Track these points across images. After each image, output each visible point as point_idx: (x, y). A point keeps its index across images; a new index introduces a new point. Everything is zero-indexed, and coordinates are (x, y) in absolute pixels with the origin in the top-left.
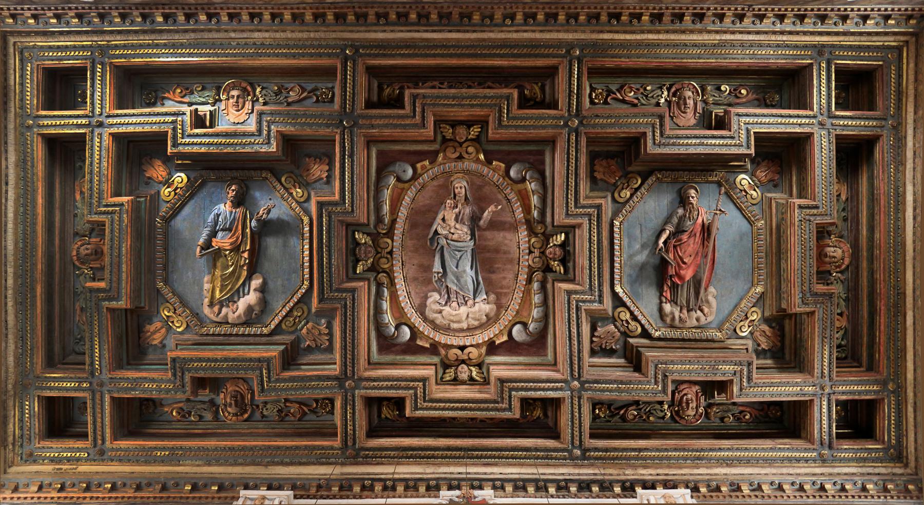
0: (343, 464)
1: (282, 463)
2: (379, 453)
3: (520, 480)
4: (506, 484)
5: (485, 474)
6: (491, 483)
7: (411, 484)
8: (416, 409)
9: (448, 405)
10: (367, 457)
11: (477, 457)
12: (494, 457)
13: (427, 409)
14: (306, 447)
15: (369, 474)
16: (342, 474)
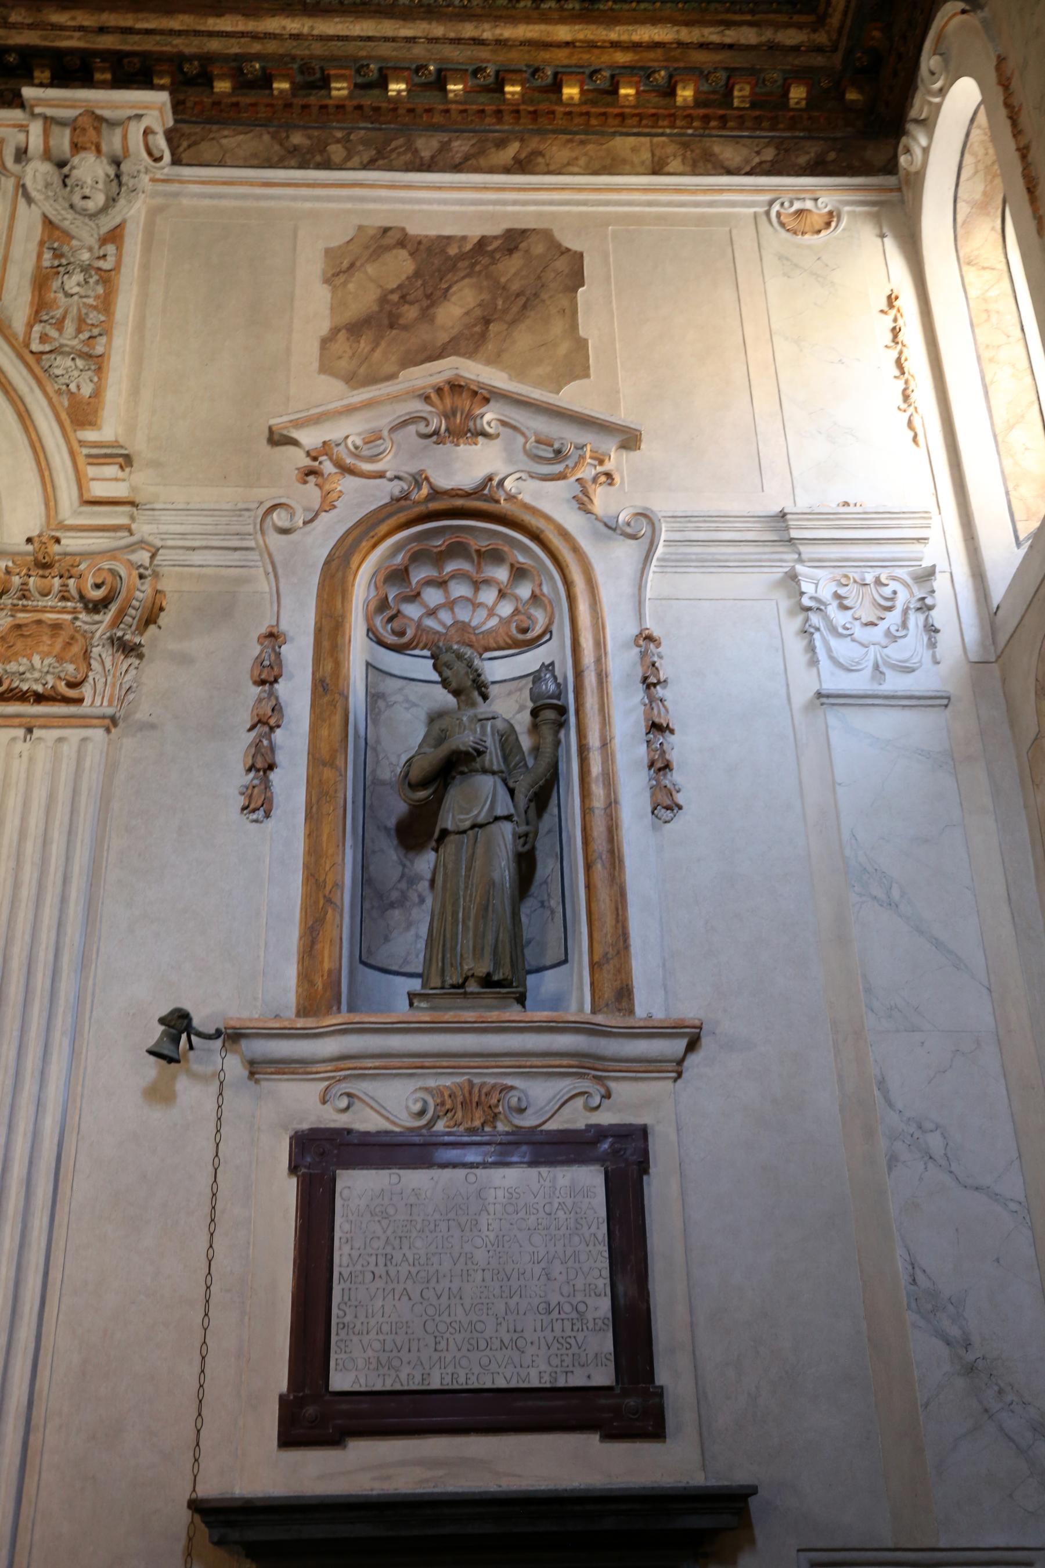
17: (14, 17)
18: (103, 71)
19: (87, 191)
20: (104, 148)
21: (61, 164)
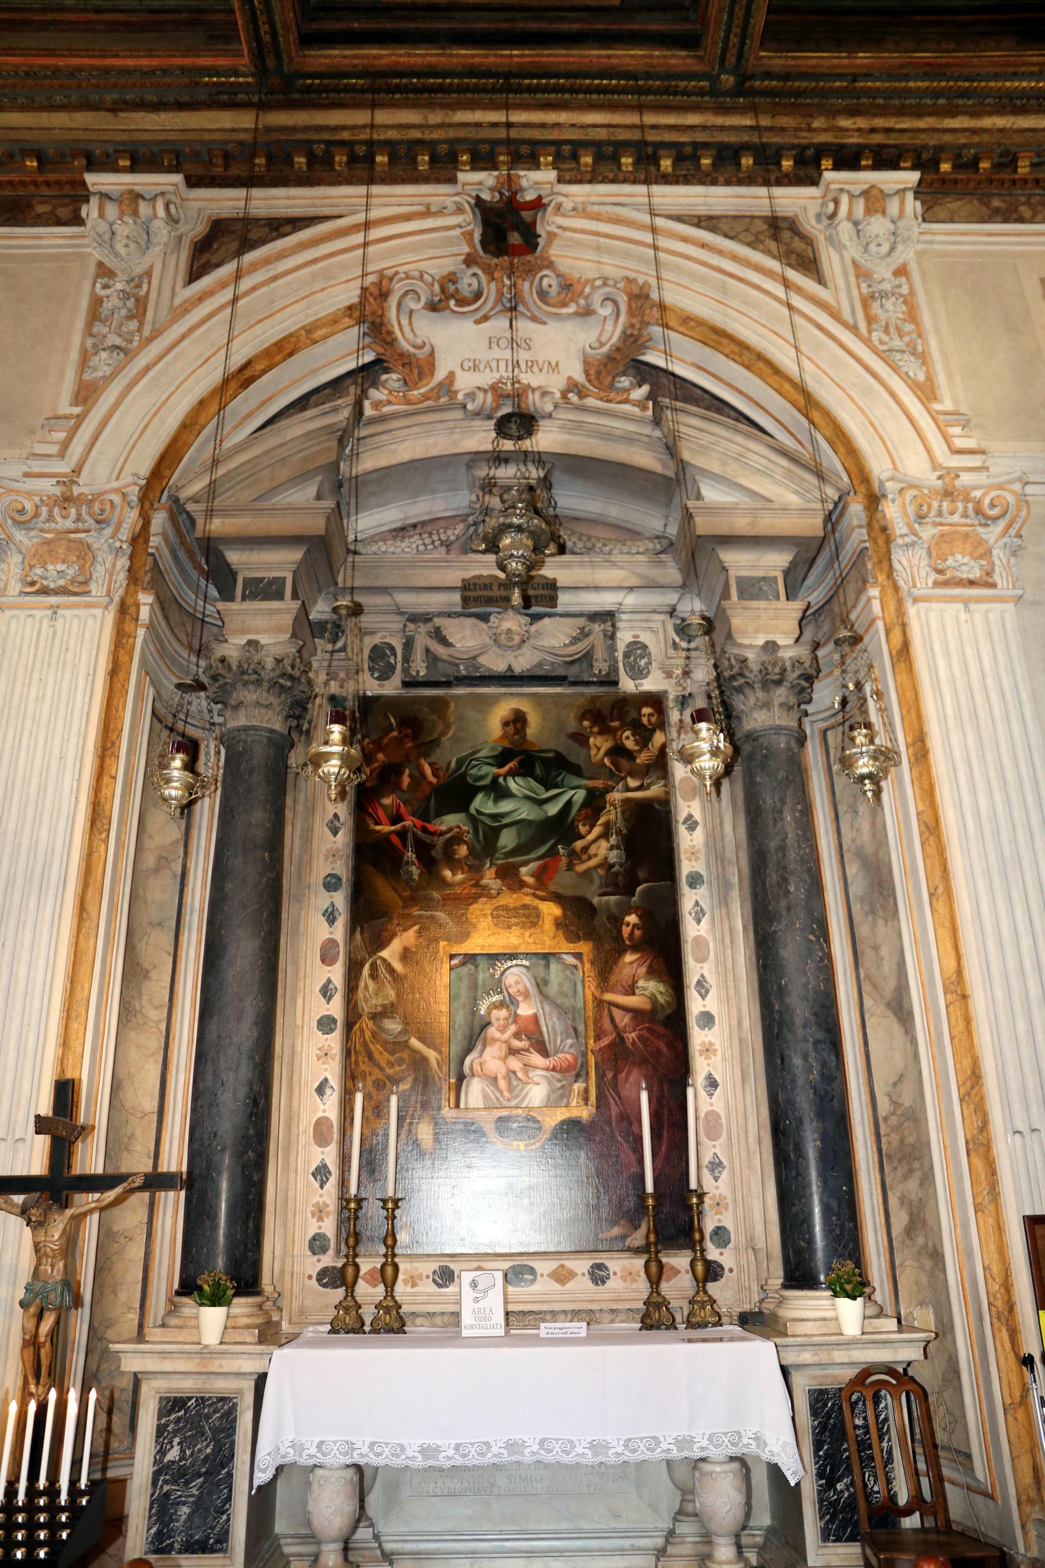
0: (262, 107)
1: (142, 106)
3: (609, 143)
5: (543, 126)
6: (552, 149)
10: (309, 89)
11: (529, 89)
12: (562, 90)
14: (183, 69)
15: (318, 129)
16: (269, 130)
21: (856, 224)
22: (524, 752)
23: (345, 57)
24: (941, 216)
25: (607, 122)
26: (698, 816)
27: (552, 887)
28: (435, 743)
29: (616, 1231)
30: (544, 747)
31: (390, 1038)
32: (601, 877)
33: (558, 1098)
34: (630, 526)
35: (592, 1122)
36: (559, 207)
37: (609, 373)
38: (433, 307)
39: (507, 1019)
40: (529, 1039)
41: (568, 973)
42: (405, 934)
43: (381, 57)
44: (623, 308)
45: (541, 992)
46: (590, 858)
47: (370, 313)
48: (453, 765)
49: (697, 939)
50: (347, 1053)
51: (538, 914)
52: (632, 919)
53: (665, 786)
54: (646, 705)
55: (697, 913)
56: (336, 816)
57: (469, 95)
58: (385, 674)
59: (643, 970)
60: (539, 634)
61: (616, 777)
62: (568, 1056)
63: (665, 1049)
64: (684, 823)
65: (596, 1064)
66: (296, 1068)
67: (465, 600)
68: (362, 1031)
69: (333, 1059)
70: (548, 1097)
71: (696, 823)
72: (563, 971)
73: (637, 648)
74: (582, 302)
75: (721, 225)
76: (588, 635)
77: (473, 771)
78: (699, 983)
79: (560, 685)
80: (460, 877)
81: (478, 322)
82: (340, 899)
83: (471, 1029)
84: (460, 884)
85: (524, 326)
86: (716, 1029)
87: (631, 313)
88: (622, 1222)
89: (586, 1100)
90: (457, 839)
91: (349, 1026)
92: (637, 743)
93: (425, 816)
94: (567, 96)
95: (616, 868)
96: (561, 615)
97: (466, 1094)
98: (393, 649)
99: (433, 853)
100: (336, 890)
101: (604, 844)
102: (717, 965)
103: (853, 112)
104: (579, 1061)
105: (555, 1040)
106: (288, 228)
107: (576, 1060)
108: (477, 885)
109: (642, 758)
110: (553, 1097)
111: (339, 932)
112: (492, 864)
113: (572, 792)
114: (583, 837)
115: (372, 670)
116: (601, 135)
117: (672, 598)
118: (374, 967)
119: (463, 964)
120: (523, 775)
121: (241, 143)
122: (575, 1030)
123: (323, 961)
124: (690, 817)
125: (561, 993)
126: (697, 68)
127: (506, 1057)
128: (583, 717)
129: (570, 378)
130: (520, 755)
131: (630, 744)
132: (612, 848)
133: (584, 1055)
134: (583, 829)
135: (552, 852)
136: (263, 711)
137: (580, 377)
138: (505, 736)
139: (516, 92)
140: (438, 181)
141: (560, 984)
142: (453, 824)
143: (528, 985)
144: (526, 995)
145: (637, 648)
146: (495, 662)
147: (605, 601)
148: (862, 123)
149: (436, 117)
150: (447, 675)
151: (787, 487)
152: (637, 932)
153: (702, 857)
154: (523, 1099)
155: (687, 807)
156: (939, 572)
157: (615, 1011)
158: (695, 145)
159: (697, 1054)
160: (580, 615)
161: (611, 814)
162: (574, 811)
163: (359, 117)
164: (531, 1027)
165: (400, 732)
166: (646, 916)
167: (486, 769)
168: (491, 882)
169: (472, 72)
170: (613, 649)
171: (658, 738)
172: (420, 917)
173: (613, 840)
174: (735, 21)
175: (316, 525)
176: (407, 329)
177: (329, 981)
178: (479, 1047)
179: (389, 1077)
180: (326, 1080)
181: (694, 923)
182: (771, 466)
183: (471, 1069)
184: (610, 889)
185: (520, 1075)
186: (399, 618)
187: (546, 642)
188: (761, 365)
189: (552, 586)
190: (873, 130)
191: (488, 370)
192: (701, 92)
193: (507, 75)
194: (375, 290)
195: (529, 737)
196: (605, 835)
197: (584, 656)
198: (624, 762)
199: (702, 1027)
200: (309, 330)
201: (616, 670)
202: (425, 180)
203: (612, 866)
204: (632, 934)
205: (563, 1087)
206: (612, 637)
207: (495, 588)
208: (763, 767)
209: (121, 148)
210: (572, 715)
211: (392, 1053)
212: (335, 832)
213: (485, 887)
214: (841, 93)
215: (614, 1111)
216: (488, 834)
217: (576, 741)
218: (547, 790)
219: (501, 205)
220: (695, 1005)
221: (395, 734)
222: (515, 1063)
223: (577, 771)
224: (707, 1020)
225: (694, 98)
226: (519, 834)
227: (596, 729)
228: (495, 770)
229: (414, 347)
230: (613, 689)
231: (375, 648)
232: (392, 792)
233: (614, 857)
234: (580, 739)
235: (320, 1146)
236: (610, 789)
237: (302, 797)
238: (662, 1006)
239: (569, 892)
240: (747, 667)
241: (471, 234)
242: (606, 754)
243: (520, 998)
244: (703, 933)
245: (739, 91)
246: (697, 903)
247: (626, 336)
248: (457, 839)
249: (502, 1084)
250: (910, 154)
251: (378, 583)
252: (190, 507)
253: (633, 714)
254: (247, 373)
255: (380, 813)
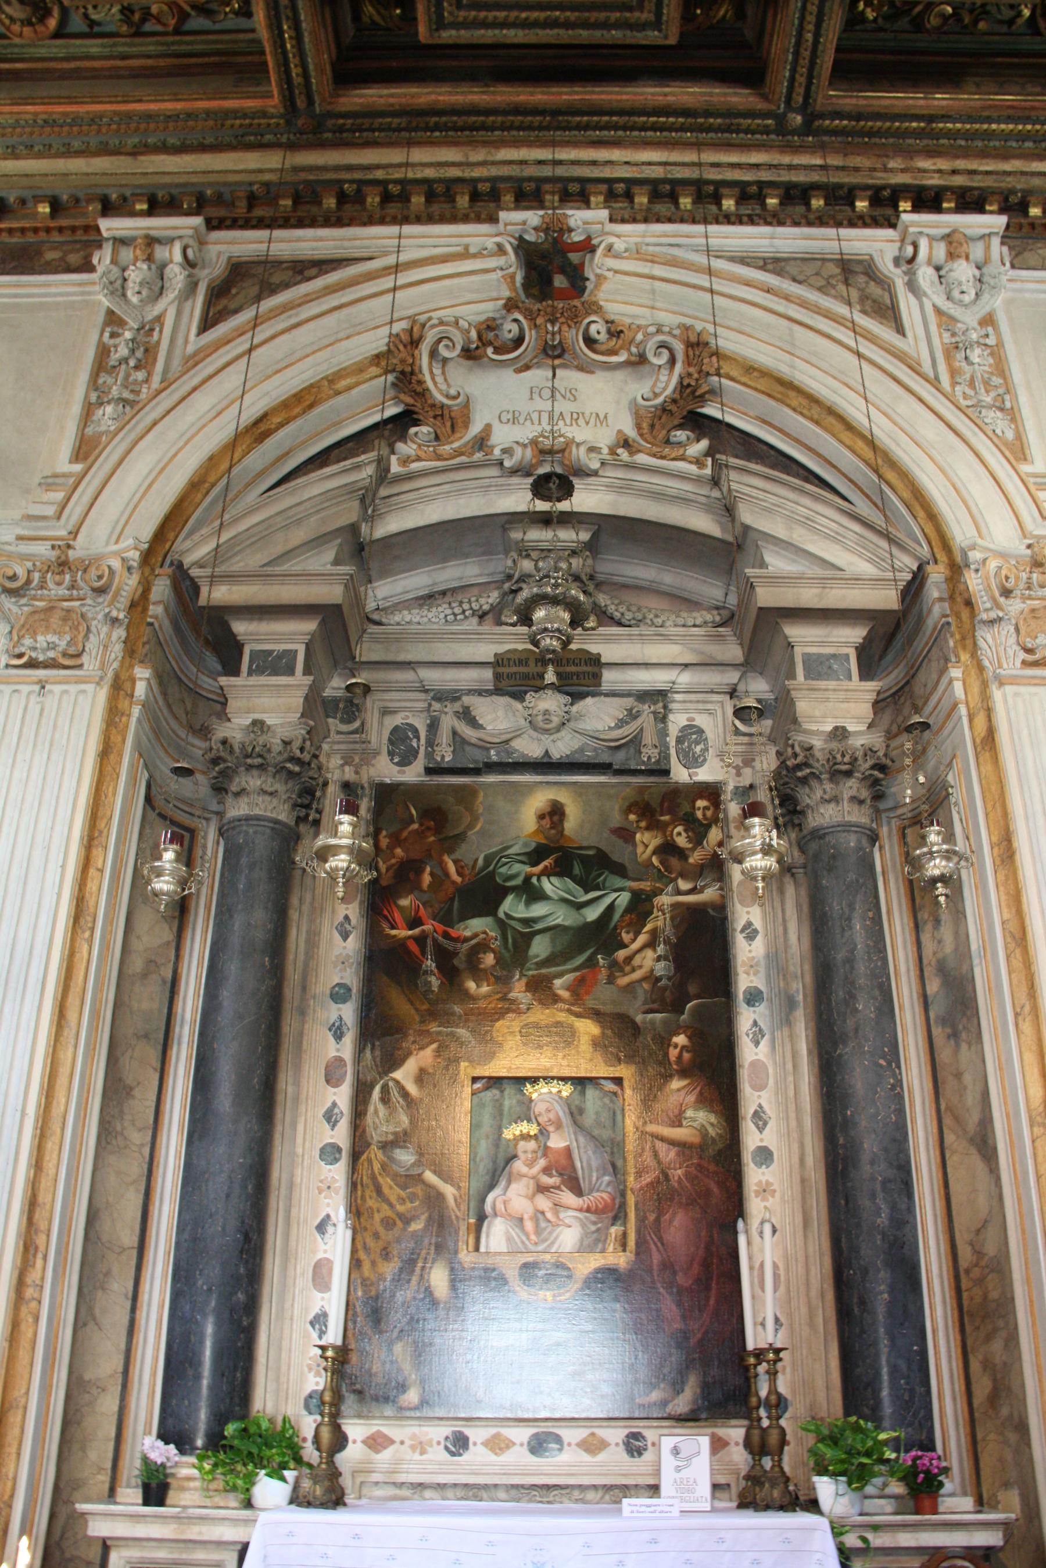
0: (292, 146)
2: (367, 122)
3: (665, 181)
4: (636, 190)
5: (594, 163)
6: (604, 187)
7: (440, 189)
8: (440, 24)
9: (514, 14)
10: (341, 129)
11: (579, 127)
12: (616, 127)
13: (465, 25)
14: (208, 113)
15: (350, 168)
16: (296, 169)
17: (892, 164)
18: (949, 201)
19: (964, 288)
20: (971, 257)
21: (938, 269)
22: (561, 849)
23: (381, 97)
24: (1032, 263)
25: (664, 159)
26: (758, 924)
27: (590, 1003)
28: (461, 837)
29: (655, 1396)
30: (585, 844)
31: (402, 1171)
32: (646, 992)
33: (593, 1243)
34: (685, 595)
35: (631, 1270)
36: (610, 248)
37: (663, 427)
38: (468, 354)
39: (535, 1152)
40: (561, 1175)
41: (607, 1100)
42: (422, 1053)
43: (419, 95)
44: (680, 357)
45: (575, 1122)
46: (633, 970)
47: (401, 363)
48: (480, 862)
49: (754, 1064)
50: (353, 1186)
51: (573, 1032)
52: (681, 1040)
53: (721, 889)
54: (701, 797)
55: (755, 1033)
56: (347, 918)
57: (514, 133)
58: (406, 759)
59: (692, 1098)
60: (580, 716)
61: (665, 877)
62: (605, 1196)
63: (716, 1190)
64: (742, 931)
65: (636, 1205)
66: (294, 1202)
67: (497, 677)
68: (370, 1161)
69: (337, 1194)
70: (582, 1241)
71: (756, 932)
72: (601, 1099)
73: (692, 733)
74: (634, 350)
75: (788, 268)
76: (635, 717)
77: (503, 870)
78: (756, 1113)
79: (604, 774)
80: (485, 989)
81: (518, 371)
82: (348, 1012)
83: (494, 1162)
84: (486, 996)
85: (568, 377)
86: (774, 1166)
87: (688, 362)
88: (662, 1386)
89: (624, 1246)
90: (483, 947)
91: (355, 1156)
92: (690, 841)
93: (446, 919)
94: (620, 133)
95: (663, 982)
96: (607, 695)
97: (488, 1236)
98: (416, 731)
99: (456, 962)
100: (344, 1001)
101: (649, 954)
102: (777, 1094)
103: (931, 153)
104: (617, 1201)
105: (590, 1176)
106: (314, 271)
107: (613, 1199)
108: (504, 998)
109: (695, 858)
110: (586, 1242)
111: (346, 1049)
112: (522, 975)
113: (615, 895)
114: (626, 946)
115: (391, 754)
116: (657, 172)
117: (732, 677)
118: (385, 1090)
119: (487, 1088)
120: (560, 874)
121: (266, 184)
122: (614, 1165)
123: (328, 1082)
124: (749, 924)
125: (598, 1123)
126: (761, 105)
127: (534, 1195)
128: (629, 810)
129: (620, 432)
130: (555, 853)
131: (682, 841)
132: (659, 959)
133: (623, 1194)
134: (626, 937)
135: (591, 963)
136: (267, 798)
137: (631, 433)
138: (537, 832)
139: (564, 129)
140: (478, 220)
141: (597, 1113)
142: (479, 929)
143: (561, 1114)
144: (559, 1126)
145: (692, 733)
146: (530, 747)
147: (657, 679)
148: (944, 164)
149: (478, 155)
150: (476, 761)
151: (860, 555)
152: (686, 1056)
153: (762, 970)
154: (553, 1243)
155: (746, 914)
156: (1029, 651)
157: (659, 1144)
158: (761, 185)
159: (753, 1195)
160: (627, 694)
161: (659, 921)
162: (617, 916)
163: (395, 156)
164: (564, 1162)
165: (421, 825)
166: (697, 1036)
167: (517, 867)
168: (521, 995)
169: (517, 110)
170: (664, 733)
171: (714, 835)
172: (439, 1033)
173: (661, 949)
174: (801, 61)
175: (332, 593)
176: (439, 379)
177: (334, 1104)
178: (503, 1183)
179: (400, 1216)
180: (328, 1216)
181: (752, 1046)
182: (841, 530)
183: (494, 1208)
184: (655, 1006)
185: (549, 1215)
186: (422, 696)
187: (590, 725)
188: (831, 420)
189: (595, 661)
190: (954, 172)
191: (528, 423)
192: (766, 131)
193: (556, 113)
194: (405, 338)
195: (567, 832)
196: (651, 944)
197: (631, 741)
198: (674, 862)
199: (759, 1164)
200: (331, 380)
201: (667, 757)
202: (465, 219)
203: (658, 979)
204: (680, 1057)
205: (598, 1230)
206: (664, 719)
207: (532, 663)
208: (830, 869)
209: (139, 191)
210: (617, 807)
211: (404, 1187)
212: (345, 936)
213: (513, 1001)
214: (919, 134)
215: (656, 1258)
216: (518, 940)
217: (620, 837)
218: (587, 892)
219: (546, 246)
220: (751, 1139)
221: (415, 826)
222: (543, 1202)
223: (620, 871)
224: (764, 1155)
225: (758, 136)
226: (553, 941)
227: (643, 824)
228: (528, 869)
229: (447, 396)
230: (663, 779)
231: (396, 730)
232: (411, 892)
233: (661, 969)
234: (625, 835)
235: (320, 1291)
236: (657, 892)
237: (308, 896)
238: (713, 1140)
239: (608, 1009)
240: (813, 756)
241: (512, 277)
242: (654, 853)
243: (551, 1129)
244: (761, 1057)
245: (807, 129)
246: (755, 1024)
247: (682, 387)
248: (483, 947)
249: (529, 1225)
250: (996, 197)
251: (402, 657)
252: (194, 572)
253: (686, 807)
254: (263, 427)
255: (397, 916)
